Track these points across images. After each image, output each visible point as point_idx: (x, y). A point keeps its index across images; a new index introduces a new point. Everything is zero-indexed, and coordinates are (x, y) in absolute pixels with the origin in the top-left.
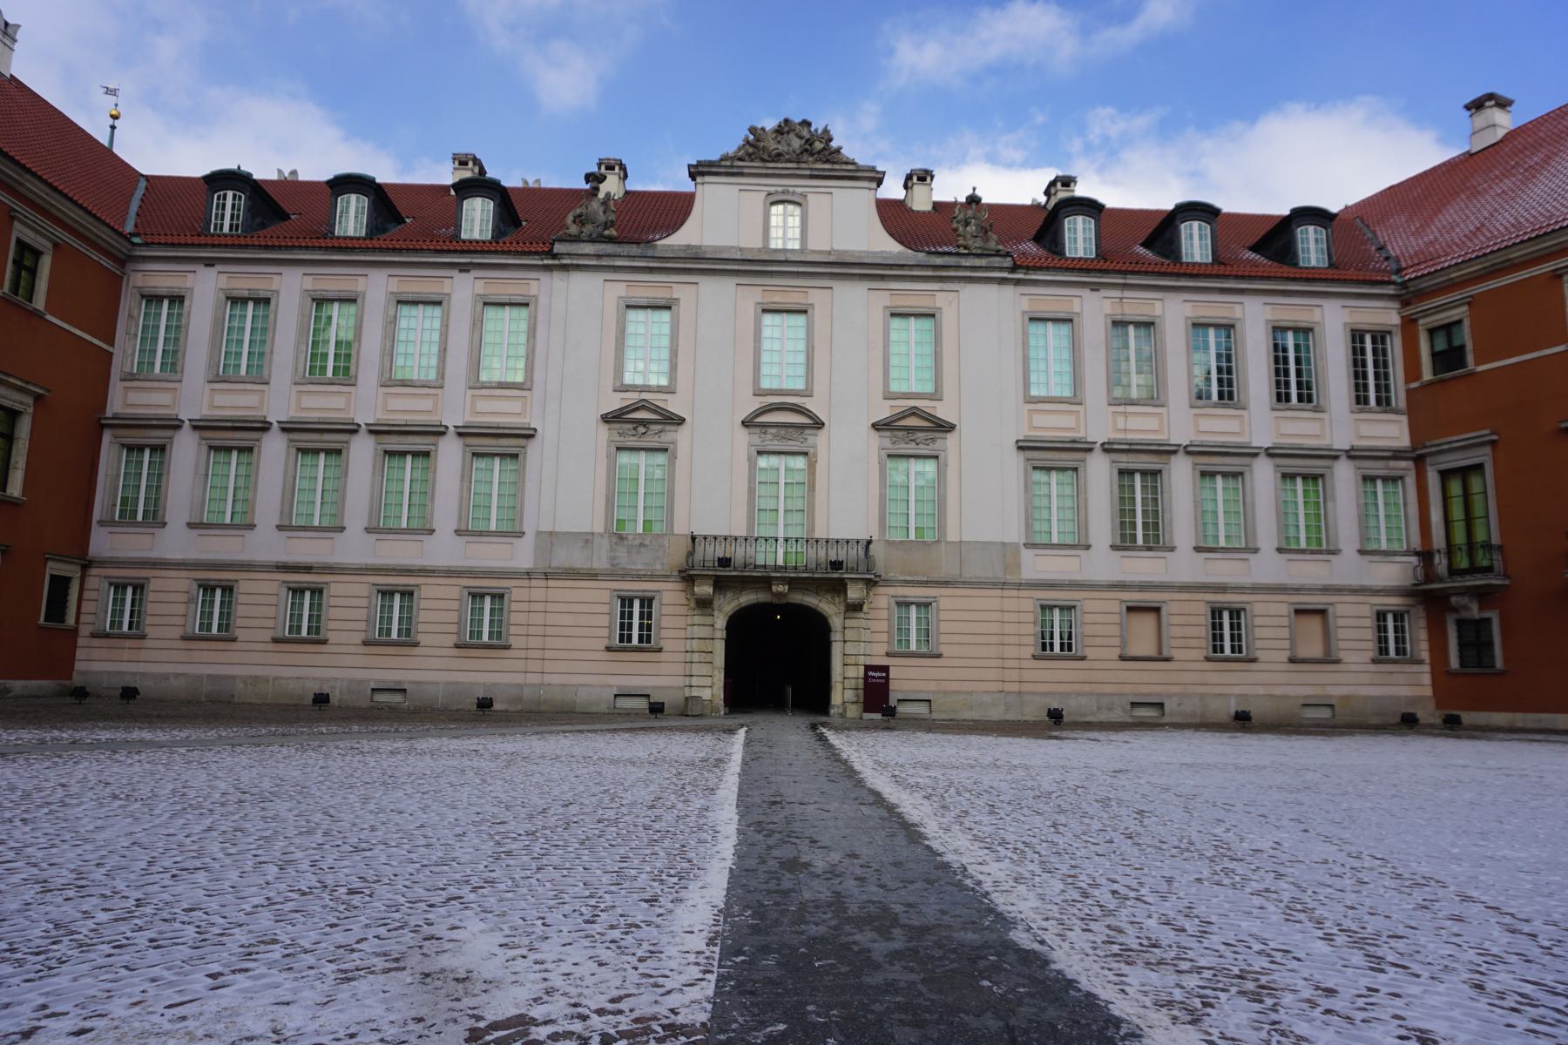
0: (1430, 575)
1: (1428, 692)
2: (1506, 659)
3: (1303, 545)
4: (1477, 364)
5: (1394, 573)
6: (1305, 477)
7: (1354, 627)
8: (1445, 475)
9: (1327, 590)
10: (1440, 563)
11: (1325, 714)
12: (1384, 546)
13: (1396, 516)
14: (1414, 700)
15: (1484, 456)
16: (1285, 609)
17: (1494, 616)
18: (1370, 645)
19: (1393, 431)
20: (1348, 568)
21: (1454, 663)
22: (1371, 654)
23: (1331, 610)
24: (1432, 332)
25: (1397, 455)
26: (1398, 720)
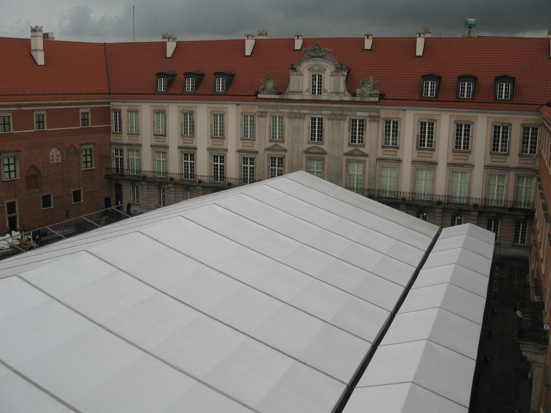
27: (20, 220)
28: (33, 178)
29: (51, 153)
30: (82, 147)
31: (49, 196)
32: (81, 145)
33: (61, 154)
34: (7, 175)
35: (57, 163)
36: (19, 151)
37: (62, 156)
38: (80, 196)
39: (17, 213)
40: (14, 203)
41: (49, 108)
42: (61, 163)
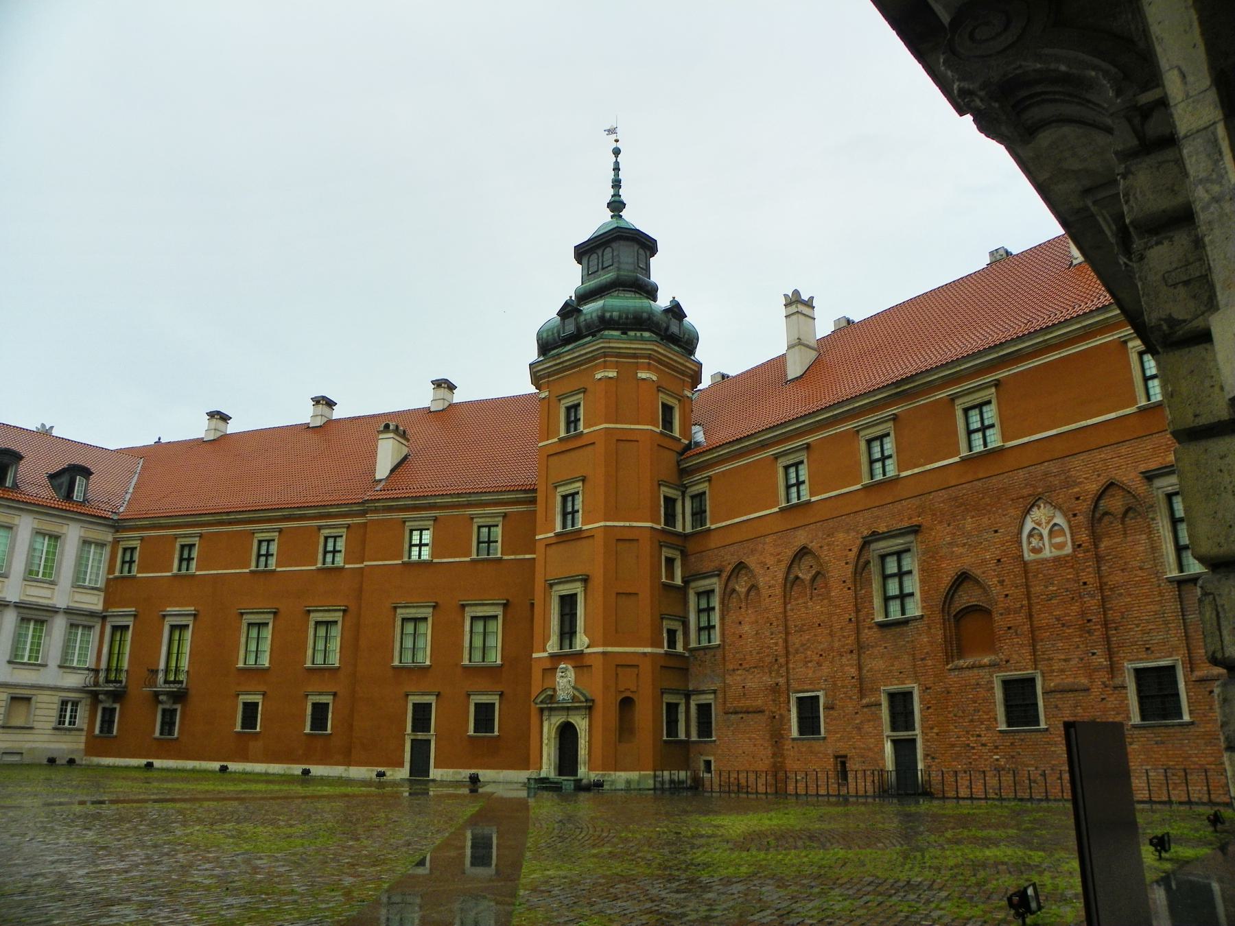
0: (96, 684)
1: (82, 746)
2: (118, 730)
3: (26, 660)
4: (138, 572)
5: (74, 680)
6: (36, 621)
7: (46, 710)
8: (115, 628)
9: (33, 687)
10: (102, 675)
11: (16, 758)
12: (75, 664)
13: (91, 649)
14: (72, 751)
15: (129, 622)
16: (4, 696)
17: (117, 706)
18: (54, 719)
19: (95, 603)
20: (51, 676)
21: (97, 731)
22: (53, 725)
23: (34, 698)
24: (125, 550)
25: (92, 614)
26: (45, 762)
27: (926, 756)
28: (964, 618)
29: (1029, 525)
30: (1159, 483)
31: (1032, 681)
32: (1149, 477)
33: (1069, 522)
34: (895, 607)
35: (1056, 559)
36: (915, 530)
37: (1070, 527)
38: (1177, 695)
39: (918, 731)
40: (908, 695)
41: (1000, 375)
42: (1073, 557)
